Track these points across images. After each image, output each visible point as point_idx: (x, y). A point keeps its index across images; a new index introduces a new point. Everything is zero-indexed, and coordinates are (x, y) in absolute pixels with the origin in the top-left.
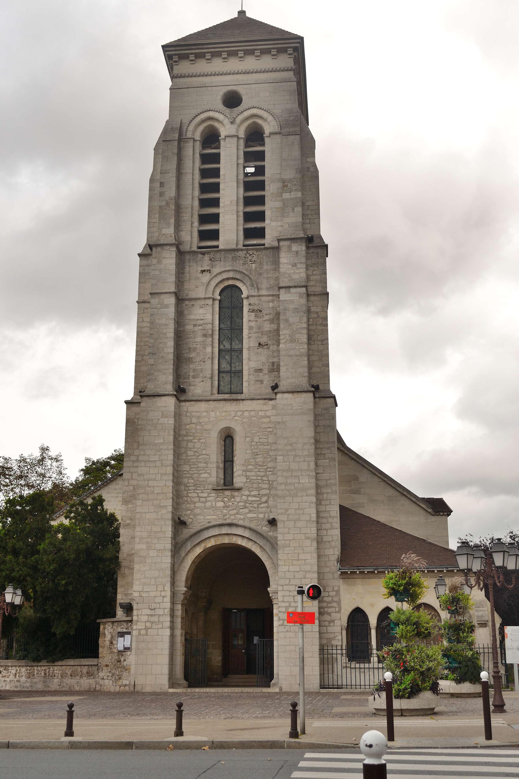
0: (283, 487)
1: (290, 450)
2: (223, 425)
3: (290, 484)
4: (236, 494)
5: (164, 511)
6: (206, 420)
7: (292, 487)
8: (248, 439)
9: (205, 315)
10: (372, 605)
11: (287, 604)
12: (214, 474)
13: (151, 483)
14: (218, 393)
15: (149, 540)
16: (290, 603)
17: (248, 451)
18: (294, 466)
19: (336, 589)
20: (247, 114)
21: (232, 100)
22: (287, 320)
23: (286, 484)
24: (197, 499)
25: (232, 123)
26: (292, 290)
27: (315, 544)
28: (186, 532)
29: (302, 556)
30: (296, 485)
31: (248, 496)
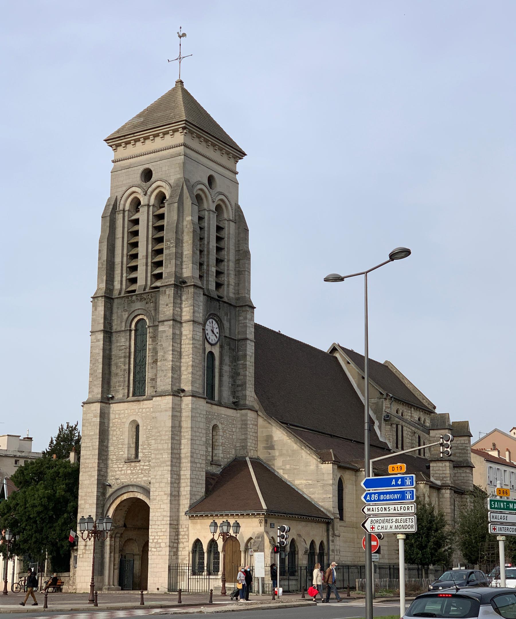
0: (154, 461)
1: (158, 436)
2: (131, 419)
3: (158, 459)
4: (138, 464)
5: (93, 479)
6: (122, 416)
7: (159, 461)
8: (144, 427)
9: (124, 343)
10: (205, 537)
11: (153, 537)
12: (126, 452)
13: (87, 461)
14: (133, 396)
15: (86, 498)
16: (155, 536)
17: (145, 436)
18: (160, 447)
19: (187, 526)
20: (154, 186)
21: (147, 175)
22: (162, 345)
23: (156, 459)
24: (117, 469)
25: (145, 195)
26: (166, 323)
27: (169, 498)
28: (110, 491)
29: (162, 506)
30: (161, 459)
31: (143, 466)
